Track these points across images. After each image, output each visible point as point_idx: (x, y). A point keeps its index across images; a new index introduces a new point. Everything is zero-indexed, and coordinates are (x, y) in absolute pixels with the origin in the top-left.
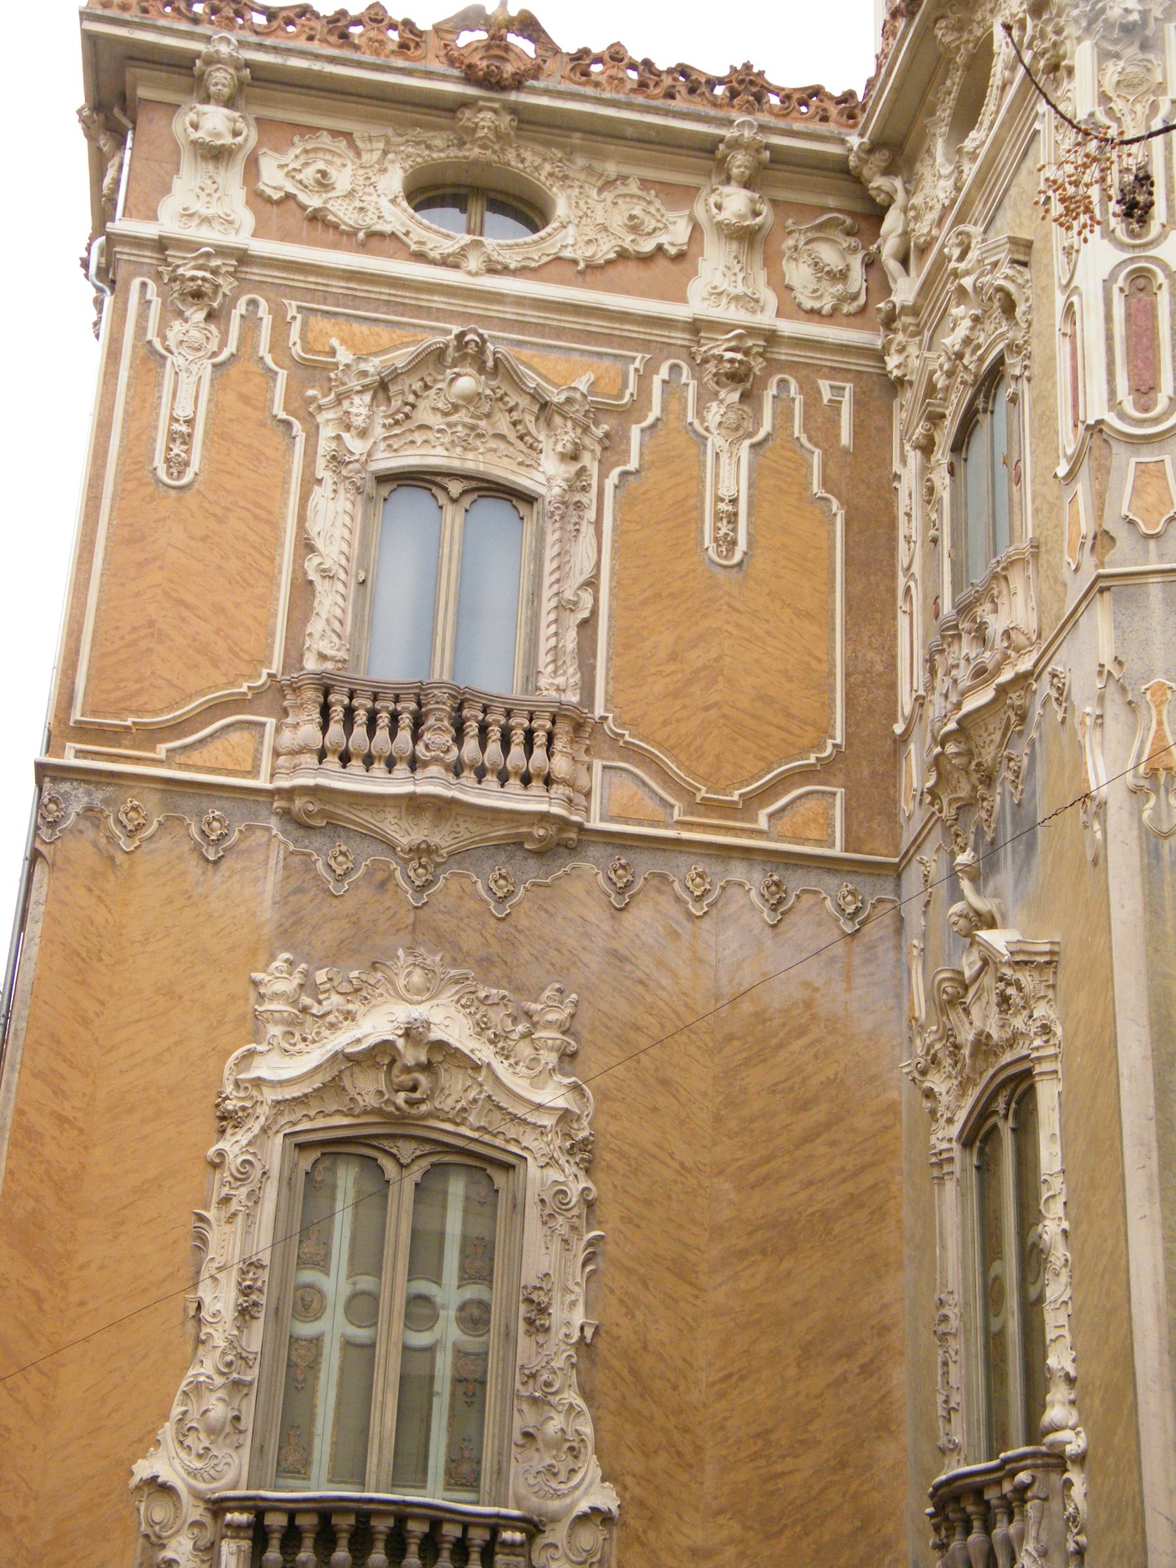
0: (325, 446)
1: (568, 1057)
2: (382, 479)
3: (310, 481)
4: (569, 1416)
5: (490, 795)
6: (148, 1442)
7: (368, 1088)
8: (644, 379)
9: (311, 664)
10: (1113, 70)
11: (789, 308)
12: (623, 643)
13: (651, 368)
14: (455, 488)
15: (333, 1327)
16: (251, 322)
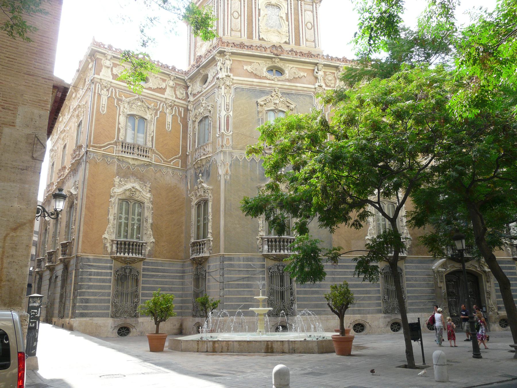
0: (121, 110)
1: (150, 191)
2: (128, 115)
3: (120, 114)
4: (150, 232)
5: (141, 158)
6: (104, 233)
7: (128, 193)
8: (160, 105)
9: (120, 139)
10: (226, 90)
11: (177, 98)
12: (156, 140)
13: (160, 103)
14: (137, 117)
15: (123, 221)
16: (112, 92)
